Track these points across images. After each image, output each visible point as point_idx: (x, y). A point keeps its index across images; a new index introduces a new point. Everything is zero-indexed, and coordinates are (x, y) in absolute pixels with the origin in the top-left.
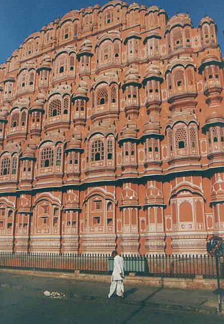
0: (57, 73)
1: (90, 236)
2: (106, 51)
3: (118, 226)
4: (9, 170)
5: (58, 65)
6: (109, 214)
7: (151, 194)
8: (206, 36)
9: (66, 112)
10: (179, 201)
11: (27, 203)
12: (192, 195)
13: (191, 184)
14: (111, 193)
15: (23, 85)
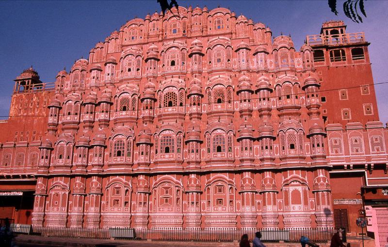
0: (168, 65)
1: (215, 214)
2: (219, 55)
3: (185, 207)
4: (124, 152)
5: (169, 58)
6: (231, 197)
7: (268, 183)
8: (308, 61)
9: (181, 105)
10: (291, 189)
11: (146, 184)
12: (301, 184)
13: (300, 176)
14: (231, 180)
15: (129, 70)
